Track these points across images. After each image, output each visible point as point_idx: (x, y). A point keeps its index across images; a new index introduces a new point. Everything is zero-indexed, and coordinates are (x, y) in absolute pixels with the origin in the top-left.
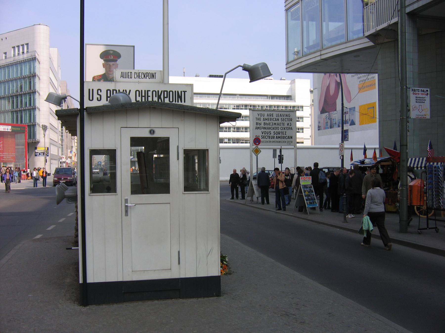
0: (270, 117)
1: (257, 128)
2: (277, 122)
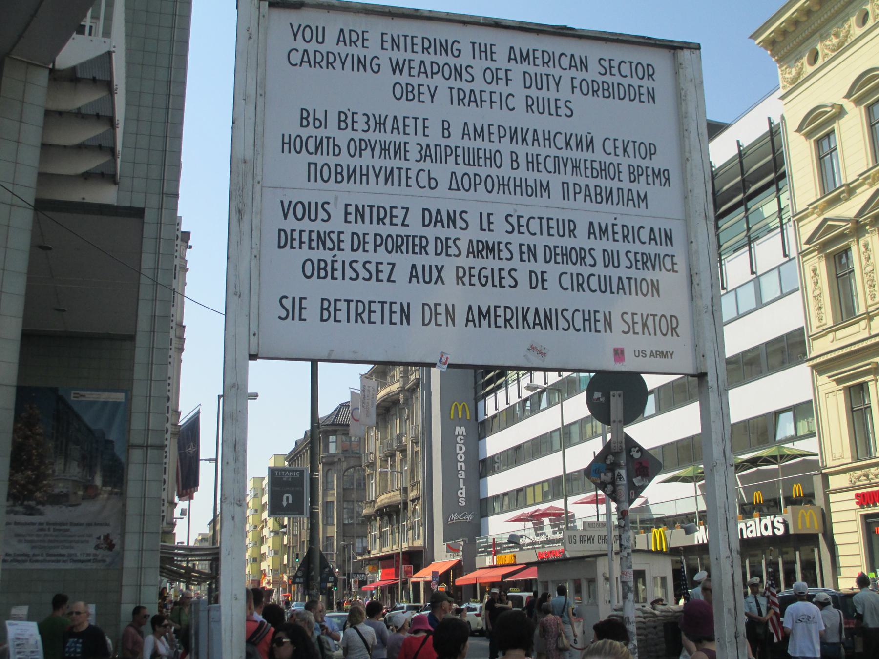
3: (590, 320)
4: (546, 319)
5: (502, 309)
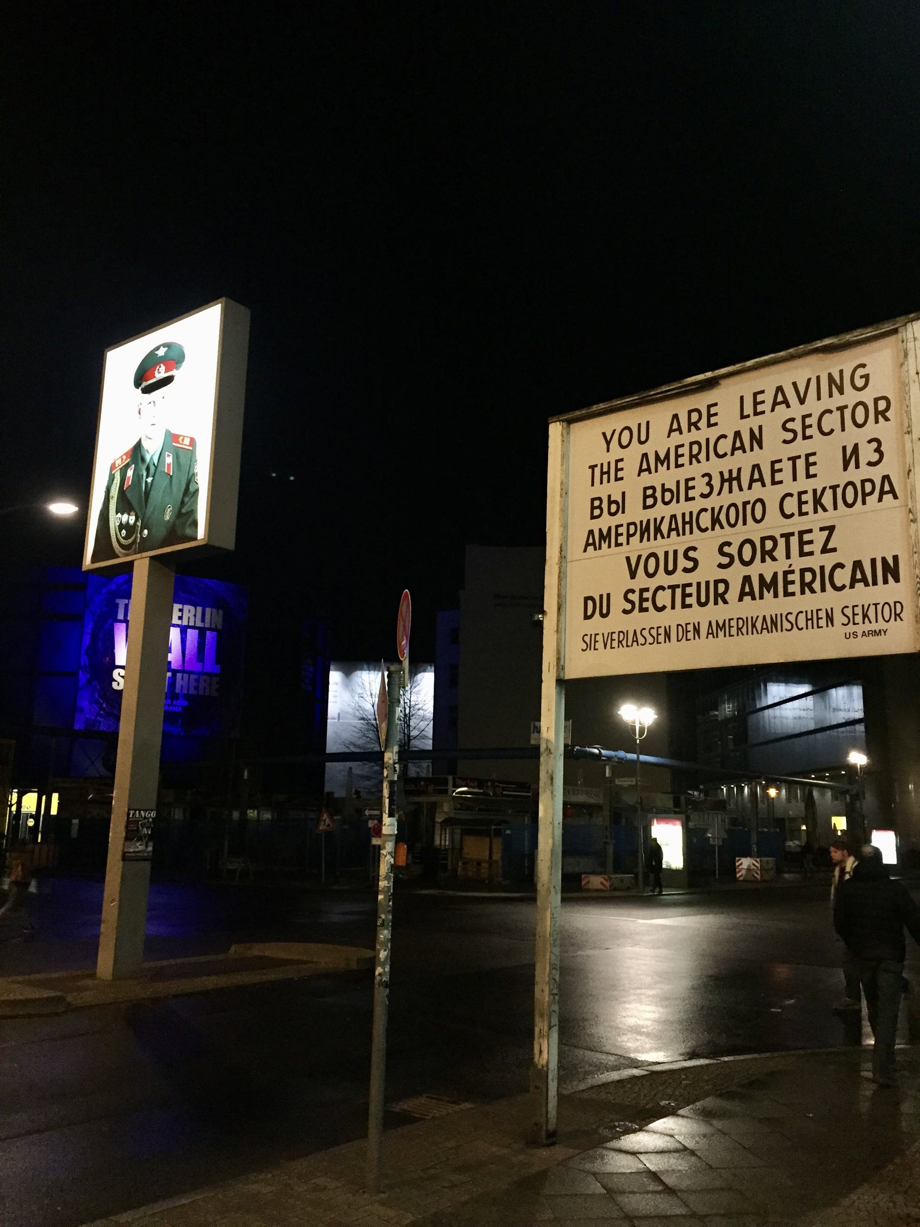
0: (687, 438)
1: (597, 540)
2: (743, 461)
3: (812, 619)
4: (773, 624)
5: (735, 621)
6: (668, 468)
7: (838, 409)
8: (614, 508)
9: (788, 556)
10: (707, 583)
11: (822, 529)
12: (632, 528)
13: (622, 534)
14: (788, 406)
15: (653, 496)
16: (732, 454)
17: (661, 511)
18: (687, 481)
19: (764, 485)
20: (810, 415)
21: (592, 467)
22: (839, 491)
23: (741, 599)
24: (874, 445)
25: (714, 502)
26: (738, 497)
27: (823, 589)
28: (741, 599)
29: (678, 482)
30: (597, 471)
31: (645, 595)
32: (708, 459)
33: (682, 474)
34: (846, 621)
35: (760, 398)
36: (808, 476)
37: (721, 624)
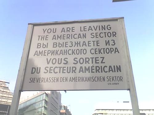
0: (66, 33)
2: (81, 40)
6: (61, 39)
7: (104, 33)
8: (44, 46)
9: (92, 63)
10: (70, 67)
11: (101, 58)
12: (49, 52)
13: (46, 53)
14: (92, 30)
15: (56, 45)
16: (78, 38)
17: (58, 48)
18: (66, 43)
19: (86, 46)
20: (97, 33)
21: (39, 36)
22: (105, 50)
23: (79, 72)
24: (113, 41)
25: (73, 48)
26: (80, 48)
27: (102, 72)
28: (79, 72)
29: (63, 43)
30: (40, 37)
31: (51, 69)
32: (72, 38)
33: (65, 41)
34: (108, 80)
35: (85, 28)
36: (97, 45)
37: (74, 78)
